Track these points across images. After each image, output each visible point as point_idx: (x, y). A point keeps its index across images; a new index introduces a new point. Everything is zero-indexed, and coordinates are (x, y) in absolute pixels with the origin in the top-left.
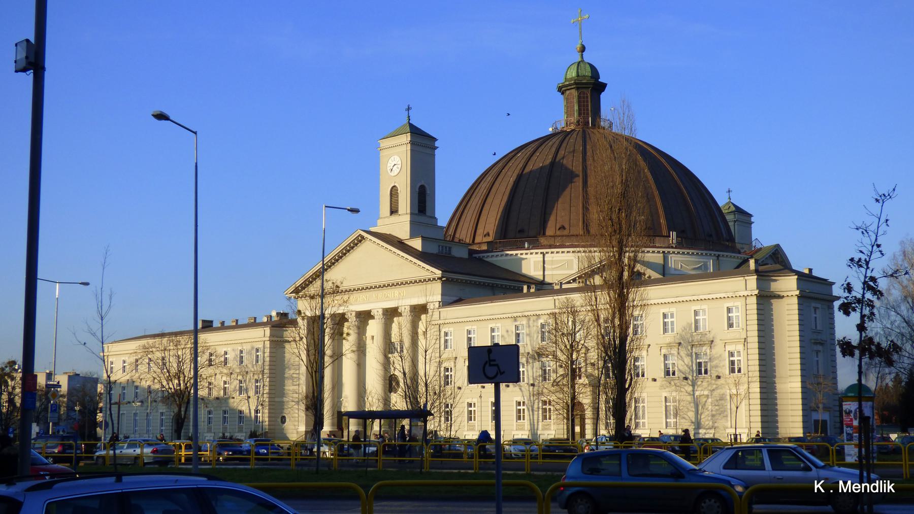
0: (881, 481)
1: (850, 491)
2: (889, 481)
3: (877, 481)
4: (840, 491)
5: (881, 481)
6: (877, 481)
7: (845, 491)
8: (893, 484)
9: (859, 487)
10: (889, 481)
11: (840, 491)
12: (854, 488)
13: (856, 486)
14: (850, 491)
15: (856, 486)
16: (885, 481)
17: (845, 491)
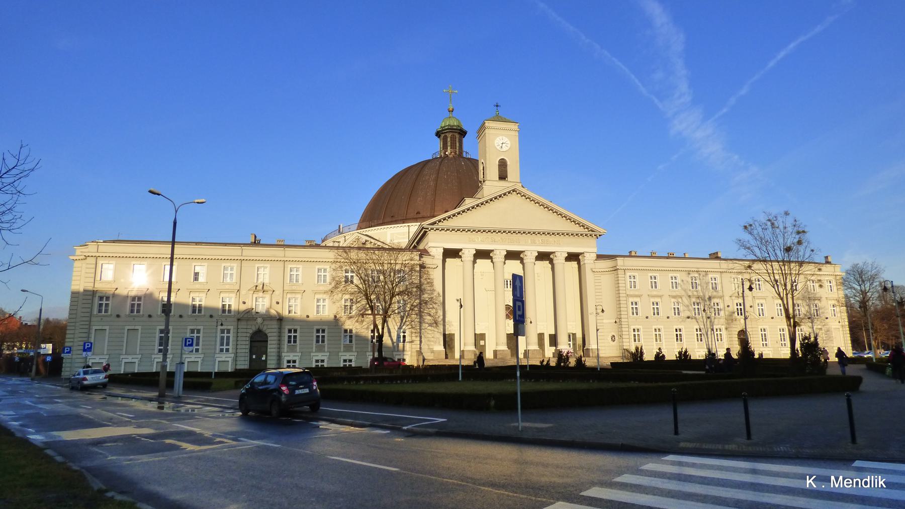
0: (873, 477)
1: (841, 486)
2: (880, 477)
3: (869, 477)
4: (832, 486)
5: (873, 477)
6: (869, 477)
7: (837, 486)
8: (884, 480)
9: (851, 482)
10: (880, 477)
11: (832, 486)
12: (845, 483)
13: (849, 481)
14: (841, 486)
15: (848, 481)
16: (876, 477)
17: (837, 486)
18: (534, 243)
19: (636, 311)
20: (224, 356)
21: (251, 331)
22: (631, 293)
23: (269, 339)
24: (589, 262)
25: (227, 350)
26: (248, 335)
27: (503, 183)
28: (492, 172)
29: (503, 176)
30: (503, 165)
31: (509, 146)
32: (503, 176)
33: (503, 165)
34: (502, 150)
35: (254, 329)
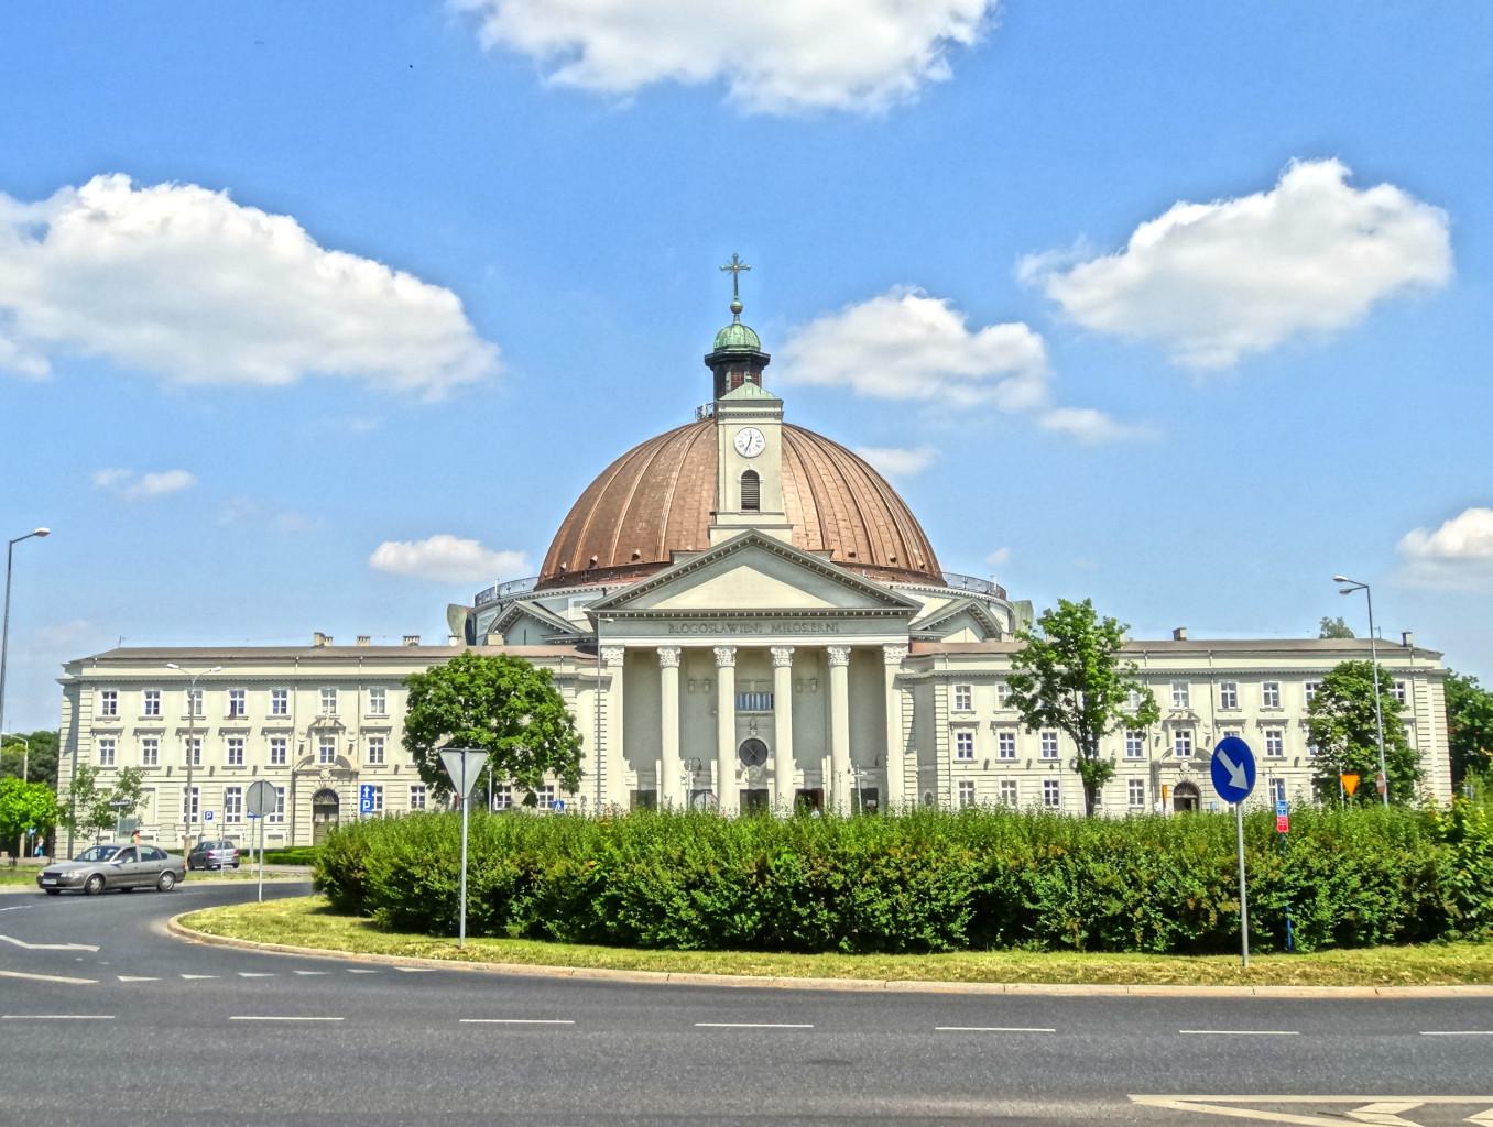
18: (788, 632)
19: (966, 750)
20: (275, 828)
21: (314, 791)
22: (957, 718)
23: (341, 801)
24: (893, 661)
25: (281, 819)
26: (310, 796)
27: (751, 519)
28: (731, 496)
29: (750, 504)
30: (751, 478)
31: (762, 445)
32: (750, 504)
33: (751, 478)
34: (747, 454)
35: (318, 786)
